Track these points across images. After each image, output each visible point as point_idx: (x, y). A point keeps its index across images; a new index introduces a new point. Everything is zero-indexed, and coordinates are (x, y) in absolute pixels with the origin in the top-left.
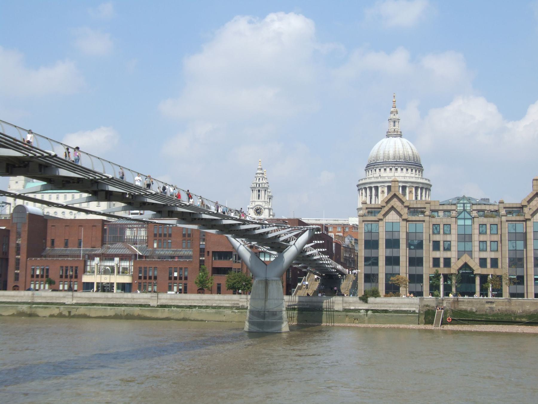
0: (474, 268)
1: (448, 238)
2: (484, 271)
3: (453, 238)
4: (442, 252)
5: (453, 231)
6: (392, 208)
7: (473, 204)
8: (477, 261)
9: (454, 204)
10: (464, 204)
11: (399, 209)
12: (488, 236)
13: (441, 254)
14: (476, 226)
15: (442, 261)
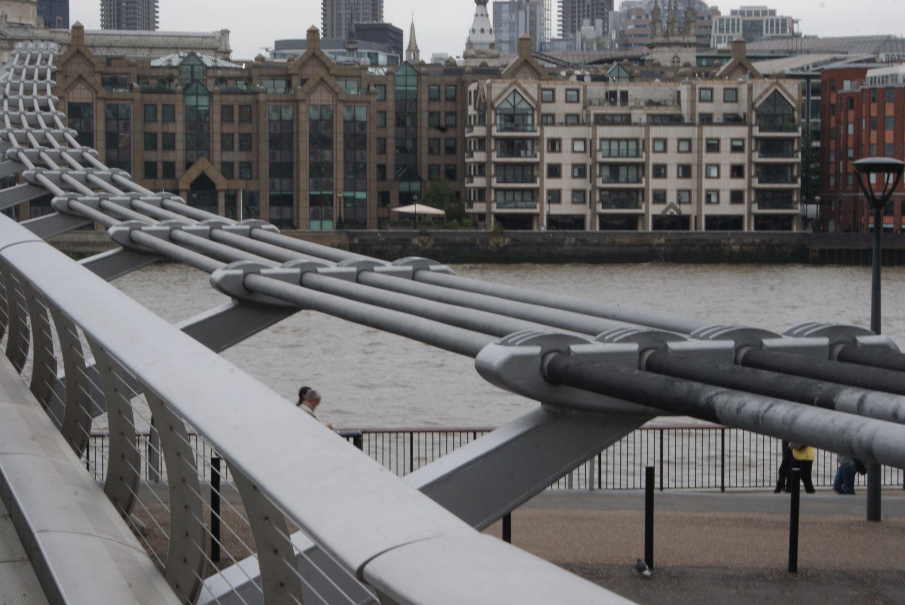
0: (216, 181)
1: (170, 128)
2: (233, 184)
3: (178, 128)
4: (160, 152)
5: (180, 117)
6: (80, 78)
7: (208, 68)
8: (218, 166)
9: (176, 68)
10: (192, 66)
11: (91, 80)
12: (236, 125)
13: (159, 156)
14: (217, 109)
15: (160, 167)
